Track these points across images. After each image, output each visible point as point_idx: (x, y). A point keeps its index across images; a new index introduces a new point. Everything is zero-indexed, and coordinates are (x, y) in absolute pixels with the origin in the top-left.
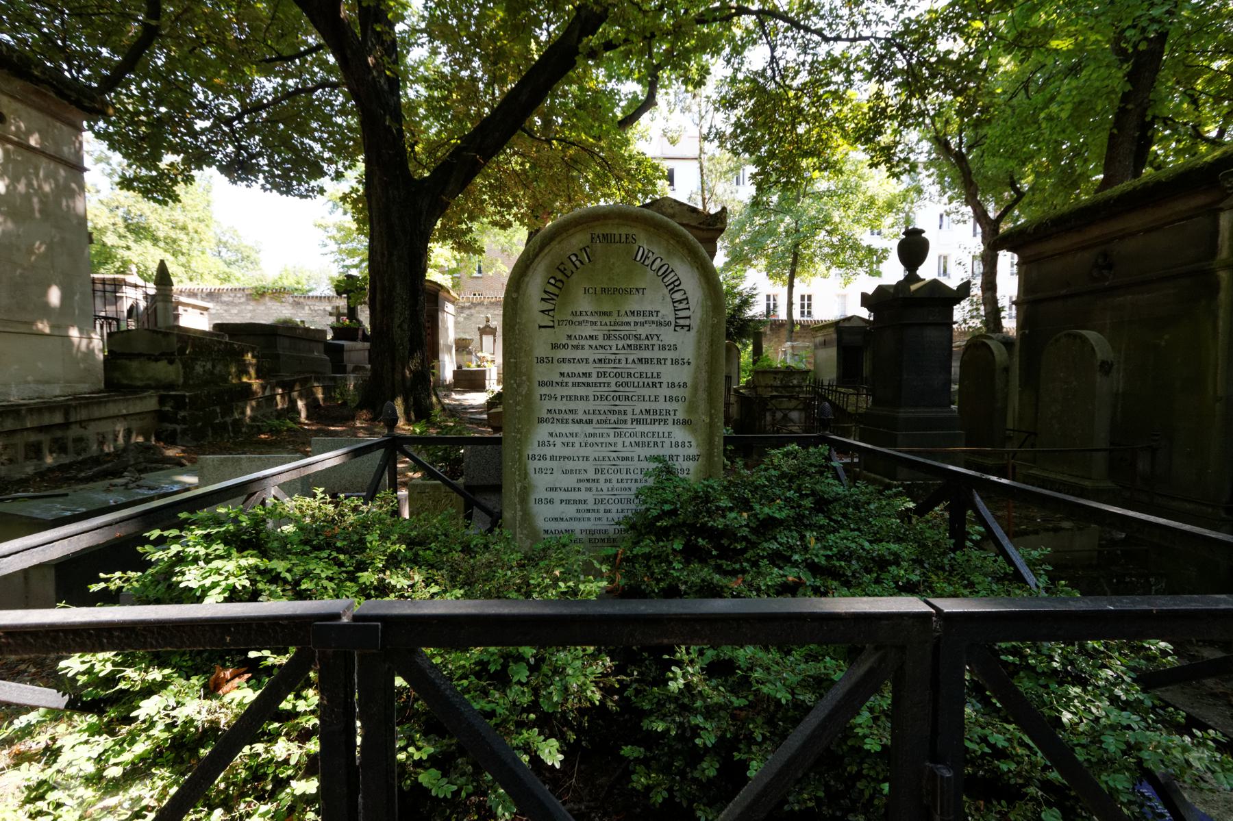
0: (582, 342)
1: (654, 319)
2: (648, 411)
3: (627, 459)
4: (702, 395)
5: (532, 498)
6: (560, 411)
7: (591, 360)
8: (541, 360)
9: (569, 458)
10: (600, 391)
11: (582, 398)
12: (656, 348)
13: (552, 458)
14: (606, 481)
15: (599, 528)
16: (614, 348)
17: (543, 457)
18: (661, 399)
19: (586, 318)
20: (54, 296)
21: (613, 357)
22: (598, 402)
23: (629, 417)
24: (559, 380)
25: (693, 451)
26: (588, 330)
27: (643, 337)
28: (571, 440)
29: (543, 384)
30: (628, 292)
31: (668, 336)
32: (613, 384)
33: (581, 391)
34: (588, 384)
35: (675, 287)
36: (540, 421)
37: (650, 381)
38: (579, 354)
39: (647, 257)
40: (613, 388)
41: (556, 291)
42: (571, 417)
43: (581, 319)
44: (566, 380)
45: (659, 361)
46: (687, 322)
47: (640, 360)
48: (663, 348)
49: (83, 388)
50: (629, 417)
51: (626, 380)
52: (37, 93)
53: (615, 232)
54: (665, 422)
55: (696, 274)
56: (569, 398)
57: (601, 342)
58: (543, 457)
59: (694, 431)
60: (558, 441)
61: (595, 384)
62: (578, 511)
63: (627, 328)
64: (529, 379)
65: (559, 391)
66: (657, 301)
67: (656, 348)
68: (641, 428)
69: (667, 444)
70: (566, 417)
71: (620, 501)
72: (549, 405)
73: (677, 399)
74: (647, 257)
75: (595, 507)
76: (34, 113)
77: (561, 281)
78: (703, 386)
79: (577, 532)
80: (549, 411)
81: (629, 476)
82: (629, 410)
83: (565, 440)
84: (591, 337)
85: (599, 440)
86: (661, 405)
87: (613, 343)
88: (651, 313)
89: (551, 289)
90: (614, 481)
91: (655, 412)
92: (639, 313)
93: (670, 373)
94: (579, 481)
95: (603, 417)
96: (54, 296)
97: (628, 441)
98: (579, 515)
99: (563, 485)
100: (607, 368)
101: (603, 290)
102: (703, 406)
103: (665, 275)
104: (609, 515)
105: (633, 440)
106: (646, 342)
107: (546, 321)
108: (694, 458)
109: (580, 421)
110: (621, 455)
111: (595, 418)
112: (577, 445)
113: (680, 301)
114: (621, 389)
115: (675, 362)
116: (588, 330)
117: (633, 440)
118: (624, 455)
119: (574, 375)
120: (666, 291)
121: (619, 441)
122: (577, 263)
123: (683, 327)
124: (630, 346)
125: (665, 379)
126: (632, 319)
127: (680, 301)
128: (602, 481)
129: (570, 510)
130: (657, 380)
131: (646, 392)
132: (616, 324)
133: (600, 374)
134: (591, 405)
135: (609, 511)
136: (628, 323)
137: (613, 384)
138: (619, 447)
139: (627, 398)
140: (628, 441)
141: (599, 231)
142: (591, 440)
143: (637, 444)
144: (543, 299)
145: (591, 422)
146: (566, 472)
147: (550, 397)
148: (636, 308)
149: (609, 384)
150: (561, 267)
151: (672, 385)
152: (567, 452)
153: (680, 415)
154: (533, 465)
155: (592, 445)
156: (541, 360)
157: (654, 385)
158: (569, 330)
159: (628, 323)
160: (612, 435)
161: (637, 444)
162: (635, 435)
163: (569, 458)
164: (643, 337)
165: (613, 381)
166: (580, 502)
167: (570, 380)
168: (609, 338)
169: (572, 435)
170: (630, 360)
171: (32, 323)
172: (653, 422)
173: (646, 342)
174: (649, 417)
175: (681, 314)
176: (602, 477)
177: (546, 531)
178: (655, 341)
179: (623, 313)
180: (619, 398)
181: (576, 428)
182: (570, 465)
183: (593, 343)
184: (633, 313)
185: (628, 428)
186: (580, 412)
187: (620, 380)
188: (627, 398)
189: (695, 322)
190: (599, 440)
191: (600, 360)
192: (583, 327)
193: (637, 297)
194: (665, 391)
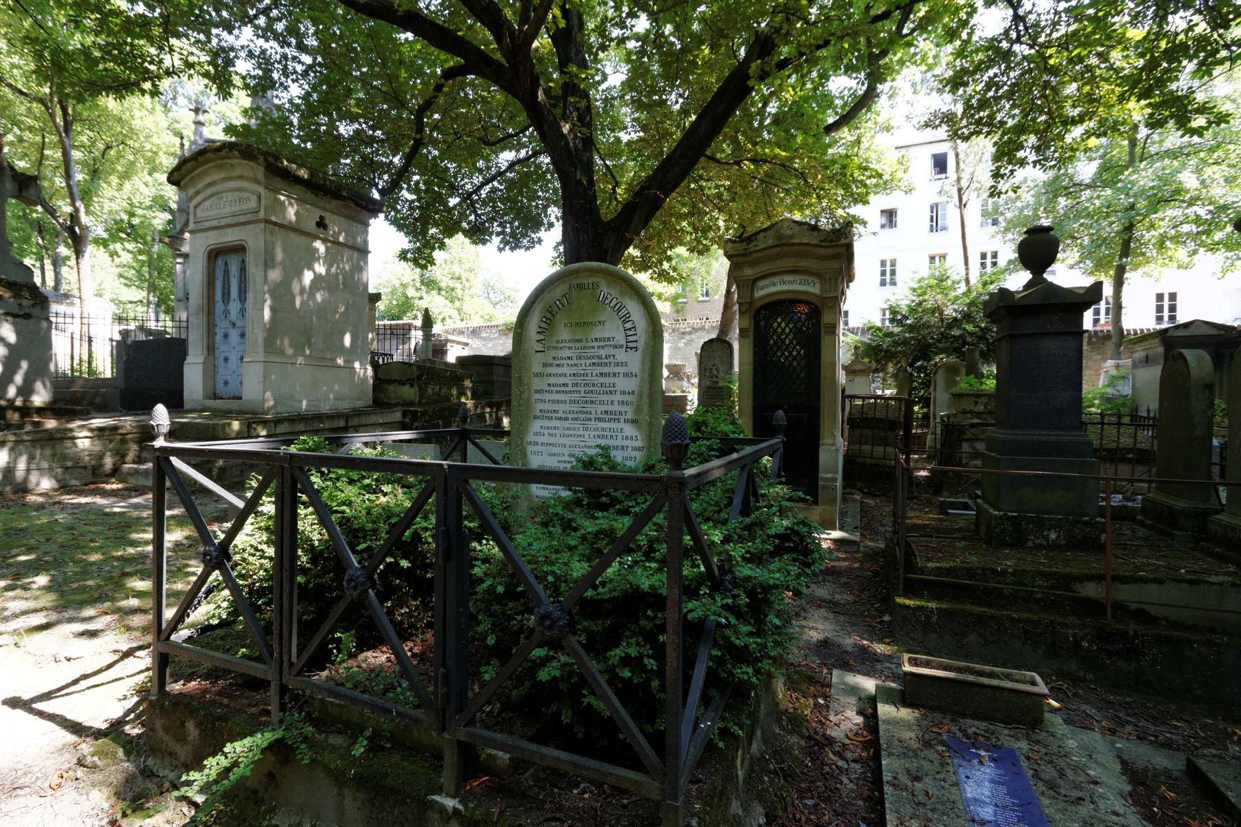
4: (646, 400)
8: (536, 375)
10: (575, 396)
17: (536, 444)
18: (616, 403)
20: (347, 340)
23: (593, 416)
25: (639, 444)
26: (566, 353)
29: (537, 392)
30: (593, 324)
31: (621, 355)
33: (561, 397)
36: (535, 417)
38: (560, 370)
42: (554, 415)
45: (614, 375)
48: (617, 364)
49: (360, 404)
52: (345, 206)
56: (554, 402)
57: (575, 361)
58: (536, 444)
59: (639, 428)
60: (546, 432)
64: (529, 389)
65: (547, 397)
66: (612, 330)
68: (601, 425)
72: (541, 406)
73: (627, 403)
76: (342, 219)
78: (646, 392)
86: (616, 408)
87: (583, 362)
89: (544, 325)
92: (601, 340)
93: (622, 384)
96: (347, 340)
100: (578, 380)
101: (577, 324)
102: (646, 408)
103: (619, 310)
105: (596, 433)
108: (639, 449)
109: (560, 419)
111: (570, 416)
115: (626, 375)
116: (566, 353)
117: (596, 433)
119: (557, 385)
121: (586, 433)
125: (619, 388)
126: (595, 344)
132: (585, 348)
134: (568, 407)
138: (586, 438)
139: (592, 402)
140: (592, 433)
141: (575, 282)
142: (567, 432)
146: (550, 455)
148: (599, 335)
151: (624, 393)
152: (552, 440)
153: (630, 416)
154: (530, 448)
156: (536, 375)
157: (611, 392)
158: (554, 353)
165: (582, 389)
167: (554, 389)
171: (334, 360)
172: (610, 420)
175: (630, 339)
181: (558, 423)
182: (554, 450)
183: (570, 362)
185: (592, 424)
188: (592, 402)
189: (641, 345)
194: (619, 397)
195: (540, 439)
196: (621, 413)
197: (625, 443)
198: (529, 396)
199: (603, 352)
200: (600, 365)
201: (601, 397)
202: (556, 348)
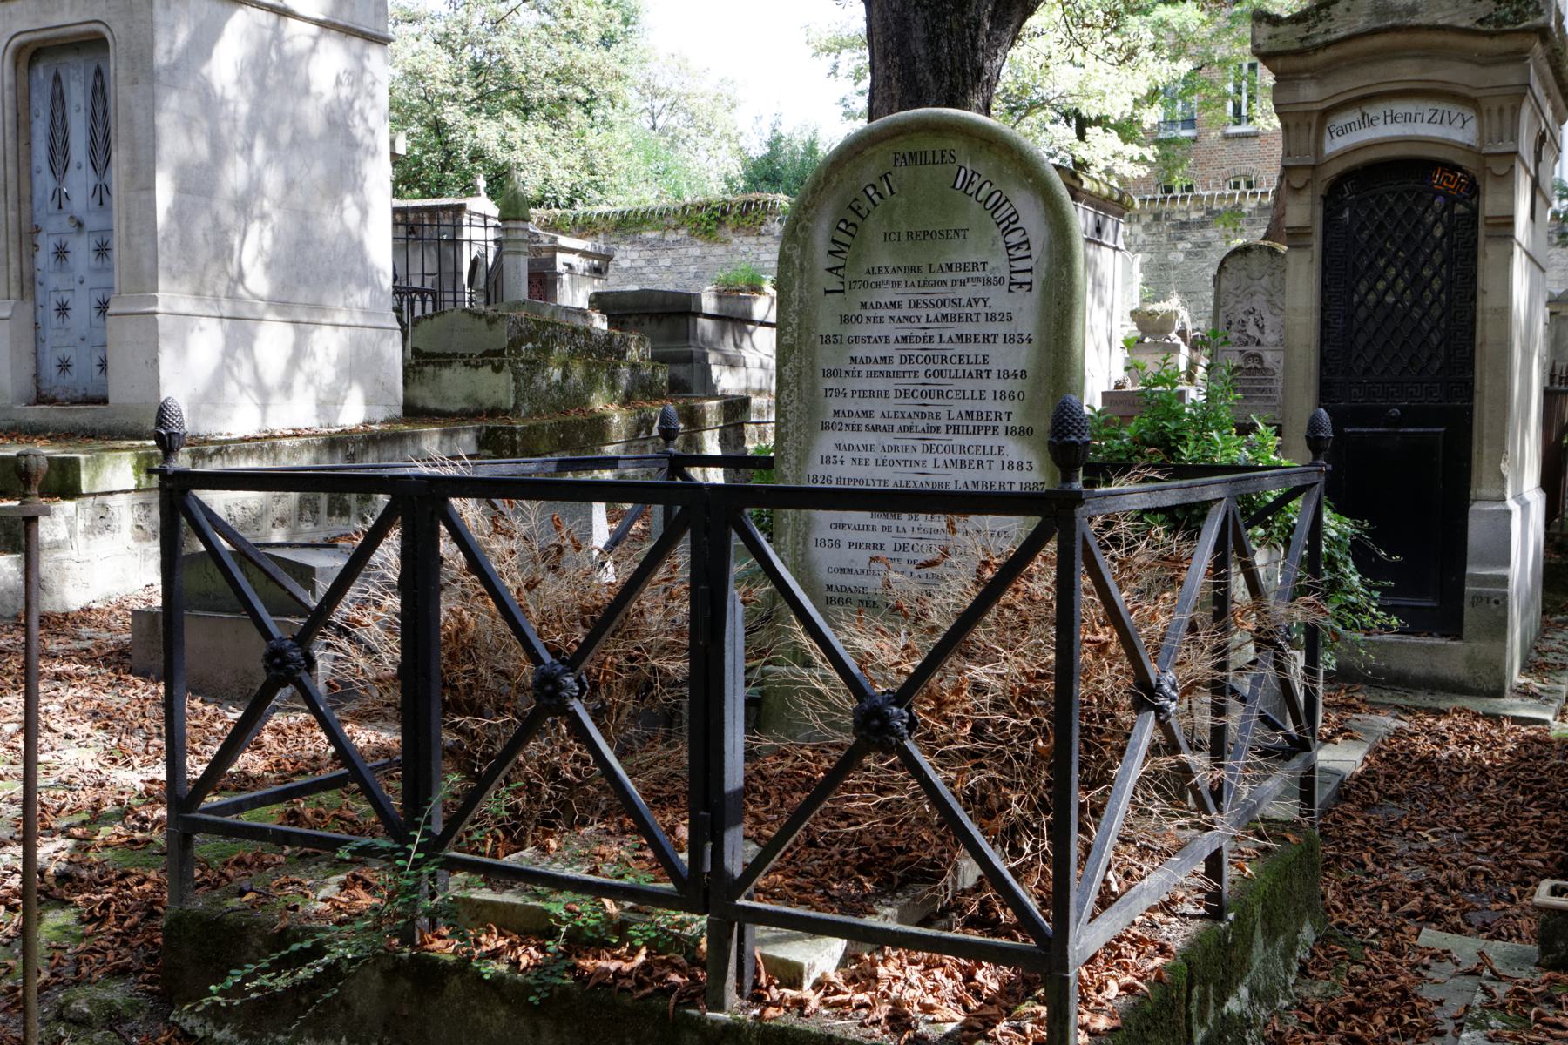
0: (881, 312)
1: (981, 274)
2: (969, 414)
8: (826, 340)
10: (905, 383)
11: (879, 394)
12: (982, 318)
16: (923, 320)
19: (887, 277)
21: (921, 333)
22: (901, 400)
23: (943, 423)
24: (850, 368)
26: (888, 295)
28: (864, 455)
30: (944, 235)
31: (999, 299)
34: (888, 374)
37: (973, 368)
42: (864, 421)
43: (879, 278)
44: (859, 367)
47: (960, 337)
48: (991, 318)
51: (940, 367)
55: (1041, 203)
56: (863, 394)
57: (905, 311)
60: (848, 456)
61: (897, 374)
63: (942, 289)
68: (959, 440)
69: (996, 465)
70: (858, 421)
72: (835, 403)
73: (1011, 396)
75: (895, 555)
77: (854, 225)
80: (836, 413)
82: (944, 415)
83: (856, 455)
84: (893, 304)
85: (902, 456)
86: (989, 405)
87: (922, 312)
88: (975, 266)
91: (980, 414)
95: (908, 422)
97: (941, 457)
100: (913, 349)
103: (996, 207)
106: (968, 310)
109: (876, 428)
111: (897, 423)
112: (872, 462)
113: (1018, 246)
115: (1009, 339)
119: (869, 360)
120: (997, 232)
121: (929, 458)
122: (876, 198)
123: (1021, 285)
124: (945, 316)
125: (994, 366)
127: (1018, 246)
129: (862, 557)
130: (982, 367)
132: (926, 283)
134: (891, 405)
136: (944, 283)
138: (929, 468)
140: (941, 457)
142: (891, 456)
148: (955, 258)
150: (855, 205)
151: (1004, 375)
153: (1015, 422)
155: (892, 463)
156: (826, 340)
157: (979, 374)
159: (944, 283)
160: (919, 449)
162: (951, 449)
165: (922, 368)
166: (875, 546)
167: (864, 368)
168: (917, 305)
169: (865, 447)
170: (945, 338)
172: (977, 431)
173: (968, 310)
174: (971, 423)
175: (1018, 265)
177: (830, 587)
178: (980, 308)
183: (896, 313)
184: (950, 267)
186: (877, 415)
187: (932, 367)
188: (940, 394)
189: (1037, 279)
190: (902, 456)
191: (904, 338)
192: (881, 291)
193: (956, 242)
196: (998, 416)
199: (964, 293)
200: (957, 318)
202: (867, 284)
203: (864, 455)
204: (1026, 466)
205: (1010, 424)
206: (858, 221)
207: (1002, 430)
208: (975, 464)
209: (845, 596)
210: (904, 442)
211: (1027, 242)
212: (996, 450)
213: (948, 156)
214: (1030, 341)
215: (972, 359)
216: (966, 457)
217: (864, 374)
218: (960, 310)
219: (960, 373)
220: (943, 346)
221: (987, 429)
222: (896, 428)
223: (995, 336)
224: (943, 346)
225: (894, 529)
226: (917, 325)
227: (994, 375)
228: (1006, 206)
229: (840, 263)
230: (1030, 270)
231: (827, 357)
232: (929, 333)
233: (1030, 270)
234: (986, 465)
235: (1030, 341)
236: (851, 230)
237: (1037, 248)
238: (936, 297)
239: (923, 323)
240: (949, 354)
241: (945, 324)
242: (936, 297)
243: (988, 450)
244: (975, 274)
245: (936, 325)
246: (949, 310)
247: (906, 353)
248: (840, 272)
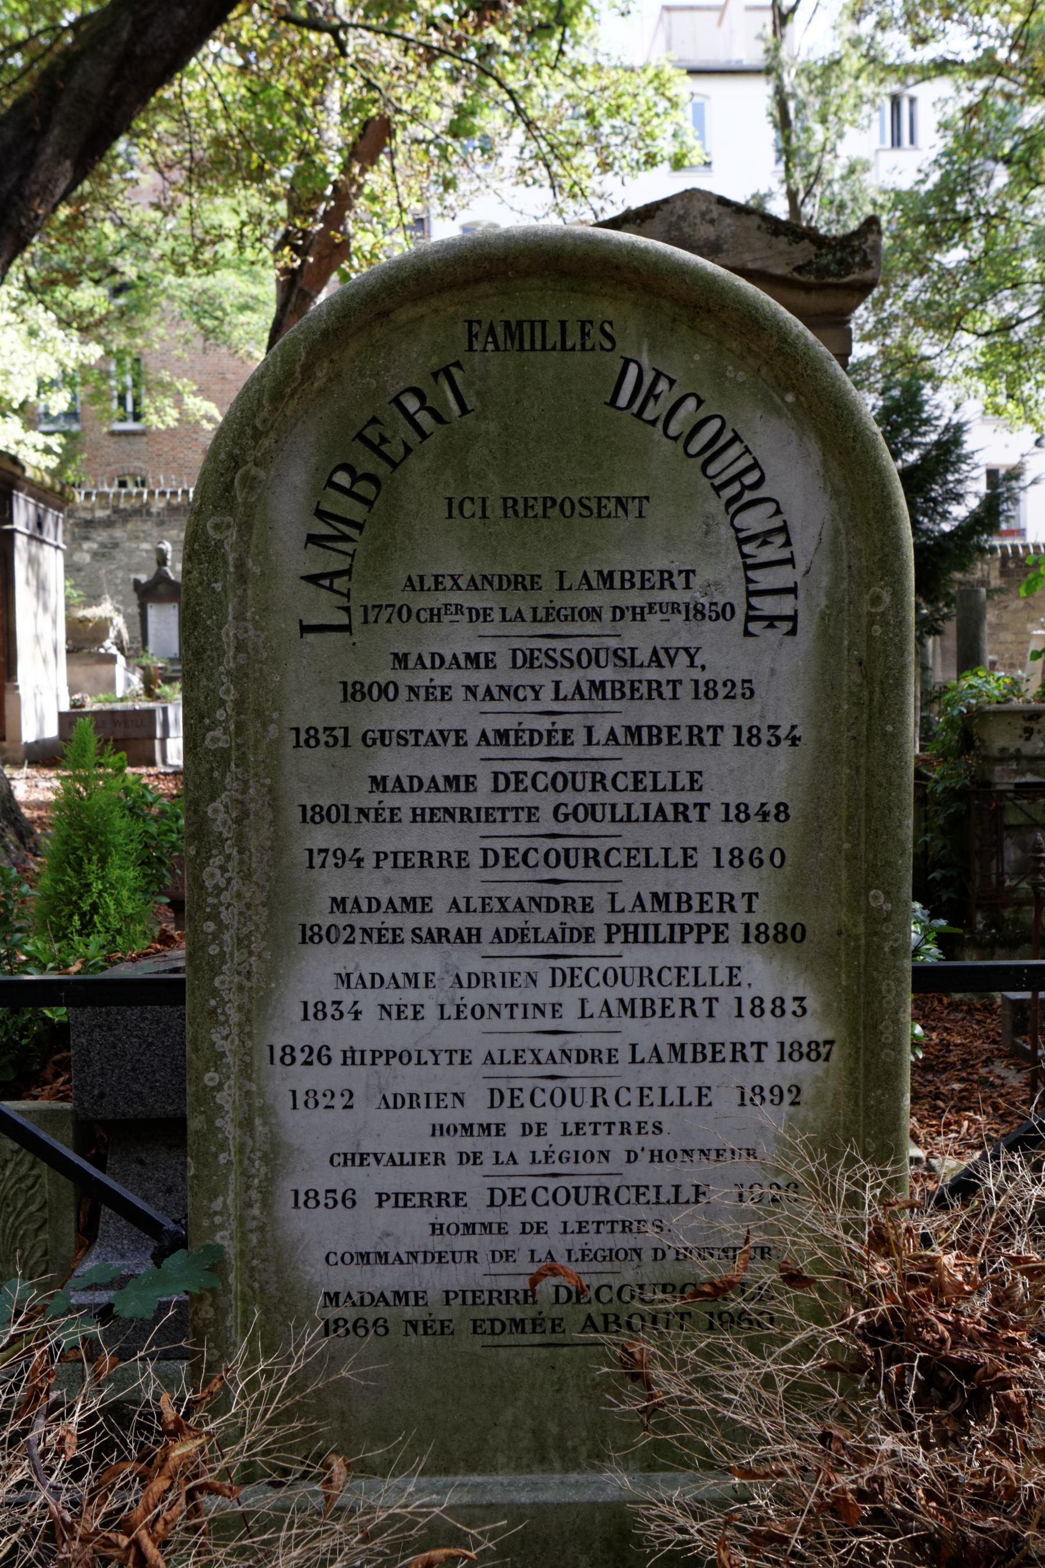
0: (442, 677)
1: (680, 596)
2: (660, 900)
3: (594, 1056)
5: (285, 1189)
6: (374, 904)
7: (473, 736)
8: (308, 738)
9: (404, 1057)
10: (505, 834)
11: (445, 859)
12: (685, 691)
13: (350, 1057)
14: (526, 1129)
15: (504, 1283)
16: (547, 693)
17: (320, 1055)
18: (705, 858)
19: (456, 598)
21: (543, 724)
22: (499, 872)
23: (599, 920)
24: (371, 801)
25: (809, 1029)
26: (458, 638)
27: (643, 655)
28: (410, 996)
30: (594, 509)
31: (723, 651)
32: (546, 813)
33: (442, 837)
34: (465, 815)
35: (743, 491)
36: (310, 935)
37: (668, 799)
38: (432, 717)
39: (652, 395)
40: (548, 824)
41: (356, 511)
42: (408, 921)
43: (438, 600)
44: (392, 800)
45: (696, 736)
46: (785, 606)
47: (634, 733)
48: (708, 690)
50: (599, 920)
51: (588, 798)
53: (546, 314)
54: (719, 933)
55: (814, 447)
56: (402, 860)
57: (504, 675)
58: (320, 1055)
60: (369, 1000)
61: (487, 814)
62: (437, 1229)
63: (590, 628)
66: (688, 543)
67: (685, 691)
68: (637, 956)
69: (725, 1008)
70: (392, 921)
71: (574, 1196)
72: (335, 882)
73: (755, 859)
74: (652, 395)
75: (492, 1216)
77: (372, 478)
79: (435, 1296)
80: (338, 904)
81: (601, 1114)
82: (600, 897)
83: (391, 997)
84: (473, 660)
85: (502, 996)
86: (706, 879)
87: (543, 678)
88: (666, 578)
90: (554, 1130)
91: (684, 901)
92: (628, 579)
93: (739, 776)
94: (439, 1130)
95: (515, 921)
97: (596, 997)
98: (439, 1244)
99: (388, 1146)
100: (525, 759)
101: (509, 505)
103: (713, 451)
104: (540, 1243)
105: (614, 993)
106: (652, 673)
107: (324, 608)
108: (814, 1051)
109: (438, 936)
110: (573, 1043)
111: (489, 923)
112: (431, 1012)
113: (763, 538)
114: (572, 827)
115: (748, 737)
117: (614, 993)
118: (587, 1043)
119: (416, 784)
120: (715, 505)
121: (569, 997)
122: (424, 419)
123: (771, 621)
124: (598, 687)
125: (714, 794)
127: (763, 538)
128: (513, 1130)
129: (412, 1227)
130: (688, 798)
131: (655, 836)
132: (552, 614)
133: (501, 782)
134: (474, 883)
135: (539, 1228)
136: (594, 613)
137: (546, 813)
138: (570, 1019)
140: (596, 997)
142: (475, 996)
143: (627, 1007)
144: (313, 539)
145: (473, 936)
146: (393, 1102)
147: (341, 858)
148: (618, 561)
149: (532, 812)
150: (372, 433)
151: (740, 813)
152: (399, 1035)
153: (765, 914)
154: (283, 1082)
155: (479, 1012)
156: (308, 738)
157: (681, 812)
159: (594, 613)
160: (544, 979)
161: (627, 1007)
162: (621, 977)
163: (404, 1057)
164: (643, 655)
165: (546, 802)
166: (442, 1199)
167: (405, 802)
168: (530, 660)
169: (412, 979)
170: (600, 734)
172: (678, 935)
173: (652, 673)
174: (664, 920)
175: (765, 579)
176: (512, 1118)
177: (332, 1298)
178: (680, 669)
179: (573, 578)
180: (565, 857)
181: (427, 958)
182: (408, 1079)
183: (480, 678)
184: (607, 579)
186: (441, 906)
187: (570, 798)
188: (592, 858)
189: (809, 609)
190: (502, 996)
191: (503, 735)
192: (444, 628)
193: (622, 525)
195: (337, 1035)
196: (727, 902)
197: (749, 1030)
198: (277, 847)
199: (641, 637)
200: (629, 691)
201: (635, 835)
202: (405, 613)
203: (410, 996)
204: (791, 1006)
205: (754, 920)
206: (382, 470)
207: (735, 932)
208: (676, 1008)
209: (370, 1314)
210: (507, 965)
211: (784, 529)
212: (722, 976)
213: (596, 336)
214: (794, 741)
215: (664, 780)
216: (655, 992)
217: (406, 815)
218: (635, 674)
219: (638, 811)
220: (595, 752)
221: (701, 930)
222: (487, 935)
223: (716, 729)
224: (595, 752)
225: (488, 1158)
226: (531, 706)
227: (714, 814)
228: (735, 450)
229: (338, 563)
230: (793, 591)
231: (309, 777)
232: (562, 723)
233: (793, 591)
234: (702, 1008)
235: (794, 741)
236: (364, 488)
237: (804, 545)
238: (576, 645)
239: (547, 701)
240: (610, 770)
241: (599, 705)
242: (576, 645)
243: (705, 976)
244: (667, 596)
245: (577, 705)
246: (608, 674)
247: (507, 767)
248: (339, 583)
